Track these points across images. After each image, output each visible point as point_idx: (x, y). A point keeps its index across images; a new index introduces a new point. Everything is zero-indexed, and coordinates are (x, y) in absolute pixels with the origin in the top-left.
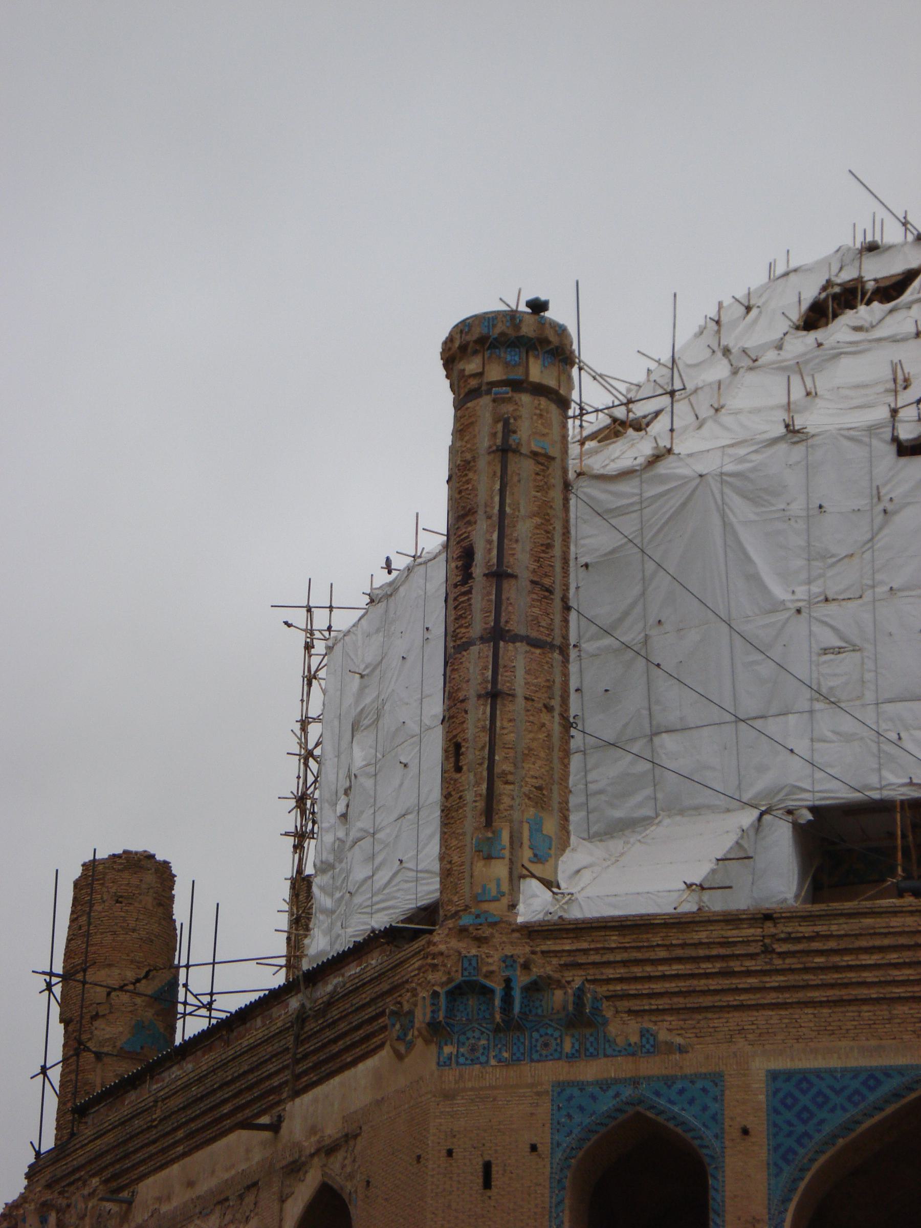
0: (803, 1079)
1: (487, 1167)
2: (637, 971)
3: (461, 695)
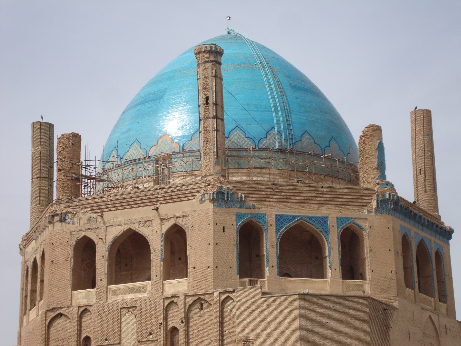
0: (281, 216)
1: (224, 227)
2: (250, 192)
3: (208, 129)
